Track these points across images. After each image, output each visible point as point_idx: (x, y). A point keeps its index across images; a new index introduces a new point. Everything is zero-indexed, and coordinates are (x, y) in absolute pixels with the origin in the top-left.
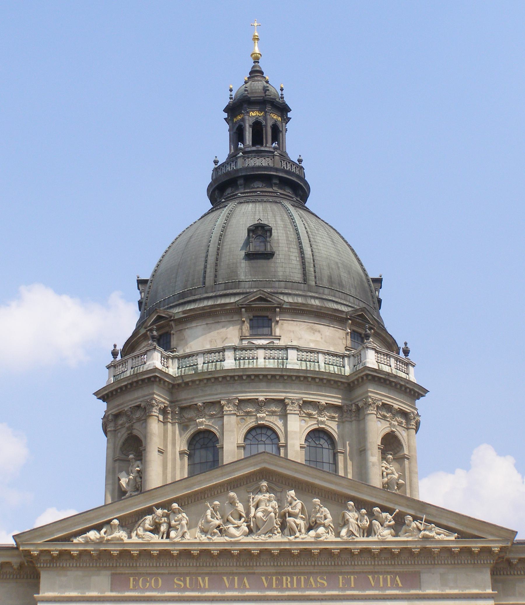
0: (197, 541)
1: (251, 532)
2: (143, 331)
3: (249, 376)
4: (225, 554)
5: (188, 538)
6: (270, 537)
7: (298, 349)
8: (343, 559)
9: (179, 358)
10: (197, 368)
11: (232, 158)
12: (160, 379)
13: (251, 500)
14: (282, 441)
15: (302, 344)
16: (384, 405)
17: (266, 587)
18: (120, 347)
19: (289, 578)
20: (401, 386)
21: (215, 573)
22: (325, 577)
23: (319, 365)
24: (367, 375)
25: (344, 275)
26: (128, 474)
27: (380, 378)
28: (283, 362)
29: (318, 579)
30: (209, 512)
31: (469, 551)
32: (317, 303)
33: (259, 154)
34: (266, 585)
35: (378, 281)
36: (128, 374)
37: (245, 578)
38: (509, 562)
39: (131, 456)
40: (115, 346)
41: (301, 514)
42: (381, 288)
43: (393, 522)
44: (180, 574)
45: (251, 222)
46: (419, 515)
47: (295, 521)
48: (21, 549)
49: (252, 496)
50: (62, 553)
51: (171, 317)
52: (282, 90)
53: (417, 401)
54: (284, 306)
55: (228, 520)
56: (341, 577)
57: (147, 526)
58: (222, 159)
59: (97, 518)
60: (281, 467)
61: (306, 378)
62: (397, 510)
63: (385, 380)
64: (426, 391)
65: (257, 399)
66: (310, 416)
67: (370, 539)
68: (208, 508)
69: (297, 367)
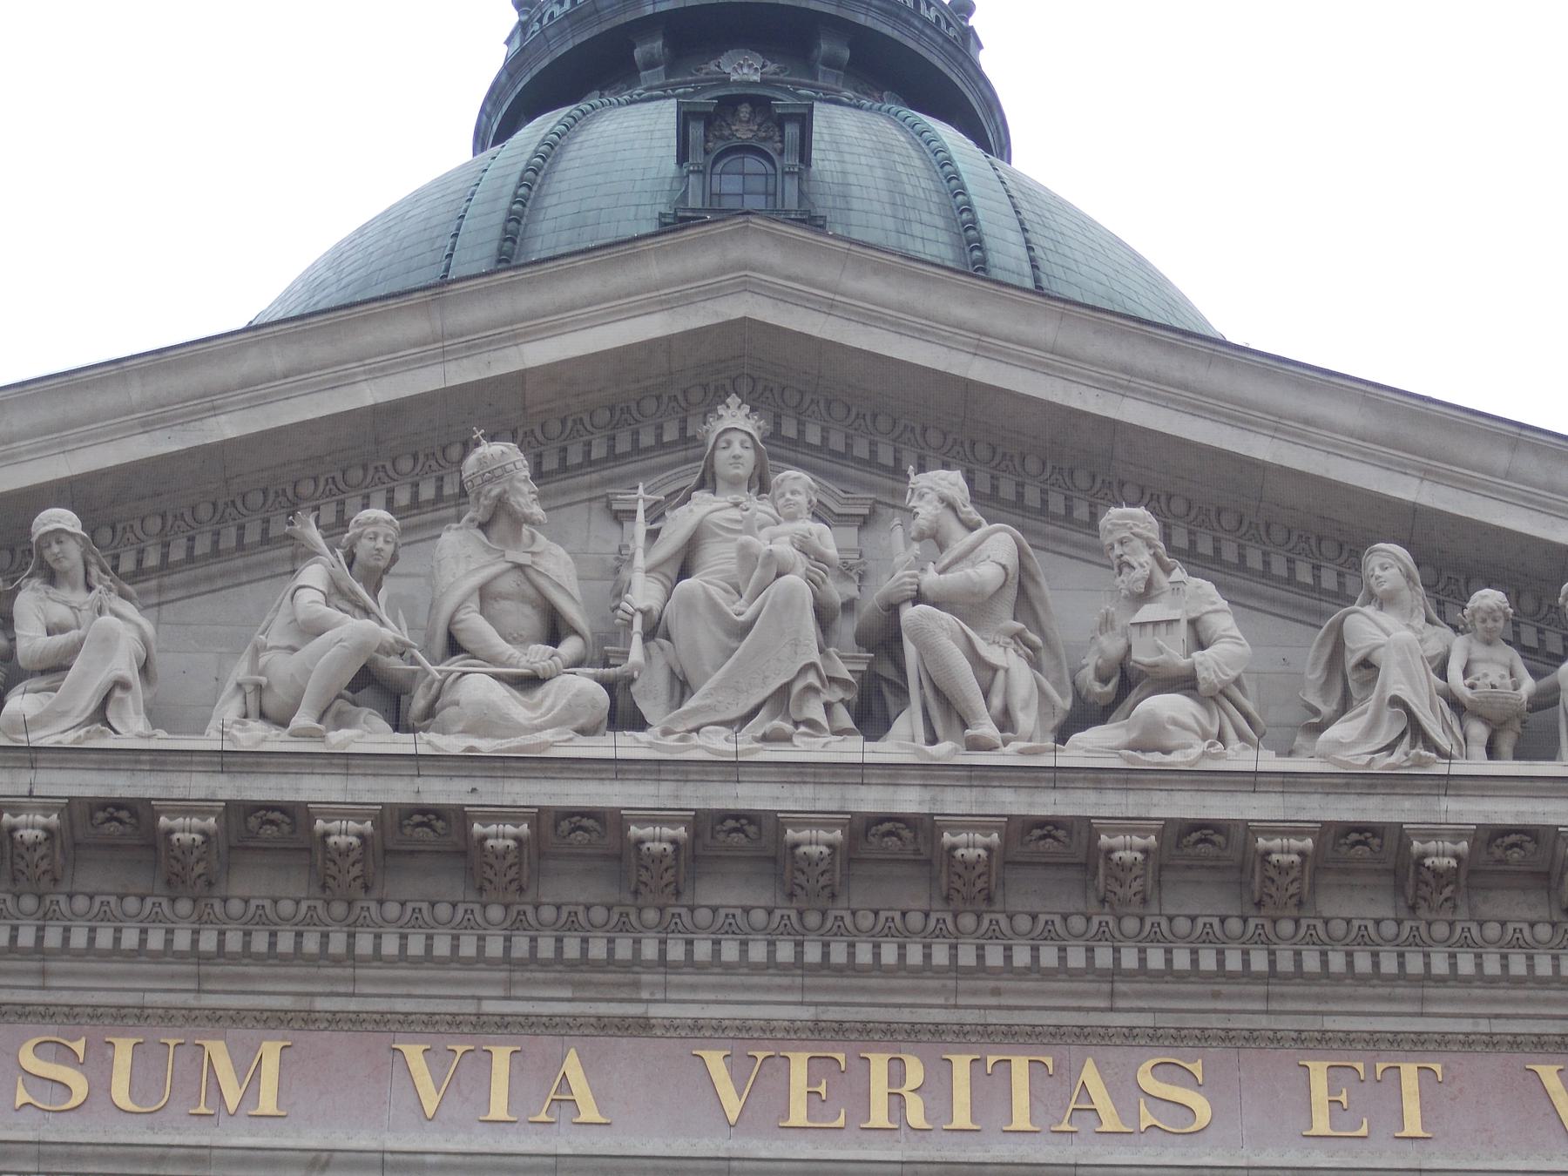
1: (624, 716)
6: (765, 738)
8: (1338, 928)
17: (732, 1118)
19: (915, 1072)
21: (334, 1020)
22: (1197, 1068)
29: (1147, 1082)
30: (313, 575)
34: (732, 1105)
37: (572, 1067)
41: (1015, 619)
47: (968, 637)
55: (454, 647)
60: (869, 318)
68: (310, 554)
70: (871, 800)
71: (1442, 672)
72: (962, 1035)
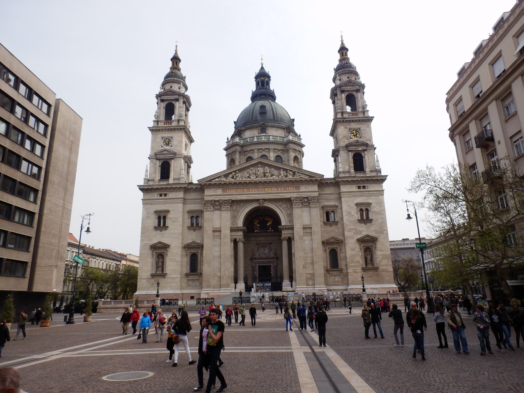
1: (257, 177)
2: (235, 134)
4: (250, 183)
5: (241, 179)
7: (272, 136)
9: (243, 139)
11: (256, 90)
14: (269, 158)
15: (274, 135)
16: (294, 149)
25: (284, 118)
33: (263, 88)
35: (293, 120)
38: (322, 183)
44: (239, 188)
45: (261, 105)
57: (231, 177)
59: (218, 175)
63: (294, 143)
64: (305, 146)
66: (276, 152)
67: (287, 178)
70: (265, 181)
72: (269, 187)
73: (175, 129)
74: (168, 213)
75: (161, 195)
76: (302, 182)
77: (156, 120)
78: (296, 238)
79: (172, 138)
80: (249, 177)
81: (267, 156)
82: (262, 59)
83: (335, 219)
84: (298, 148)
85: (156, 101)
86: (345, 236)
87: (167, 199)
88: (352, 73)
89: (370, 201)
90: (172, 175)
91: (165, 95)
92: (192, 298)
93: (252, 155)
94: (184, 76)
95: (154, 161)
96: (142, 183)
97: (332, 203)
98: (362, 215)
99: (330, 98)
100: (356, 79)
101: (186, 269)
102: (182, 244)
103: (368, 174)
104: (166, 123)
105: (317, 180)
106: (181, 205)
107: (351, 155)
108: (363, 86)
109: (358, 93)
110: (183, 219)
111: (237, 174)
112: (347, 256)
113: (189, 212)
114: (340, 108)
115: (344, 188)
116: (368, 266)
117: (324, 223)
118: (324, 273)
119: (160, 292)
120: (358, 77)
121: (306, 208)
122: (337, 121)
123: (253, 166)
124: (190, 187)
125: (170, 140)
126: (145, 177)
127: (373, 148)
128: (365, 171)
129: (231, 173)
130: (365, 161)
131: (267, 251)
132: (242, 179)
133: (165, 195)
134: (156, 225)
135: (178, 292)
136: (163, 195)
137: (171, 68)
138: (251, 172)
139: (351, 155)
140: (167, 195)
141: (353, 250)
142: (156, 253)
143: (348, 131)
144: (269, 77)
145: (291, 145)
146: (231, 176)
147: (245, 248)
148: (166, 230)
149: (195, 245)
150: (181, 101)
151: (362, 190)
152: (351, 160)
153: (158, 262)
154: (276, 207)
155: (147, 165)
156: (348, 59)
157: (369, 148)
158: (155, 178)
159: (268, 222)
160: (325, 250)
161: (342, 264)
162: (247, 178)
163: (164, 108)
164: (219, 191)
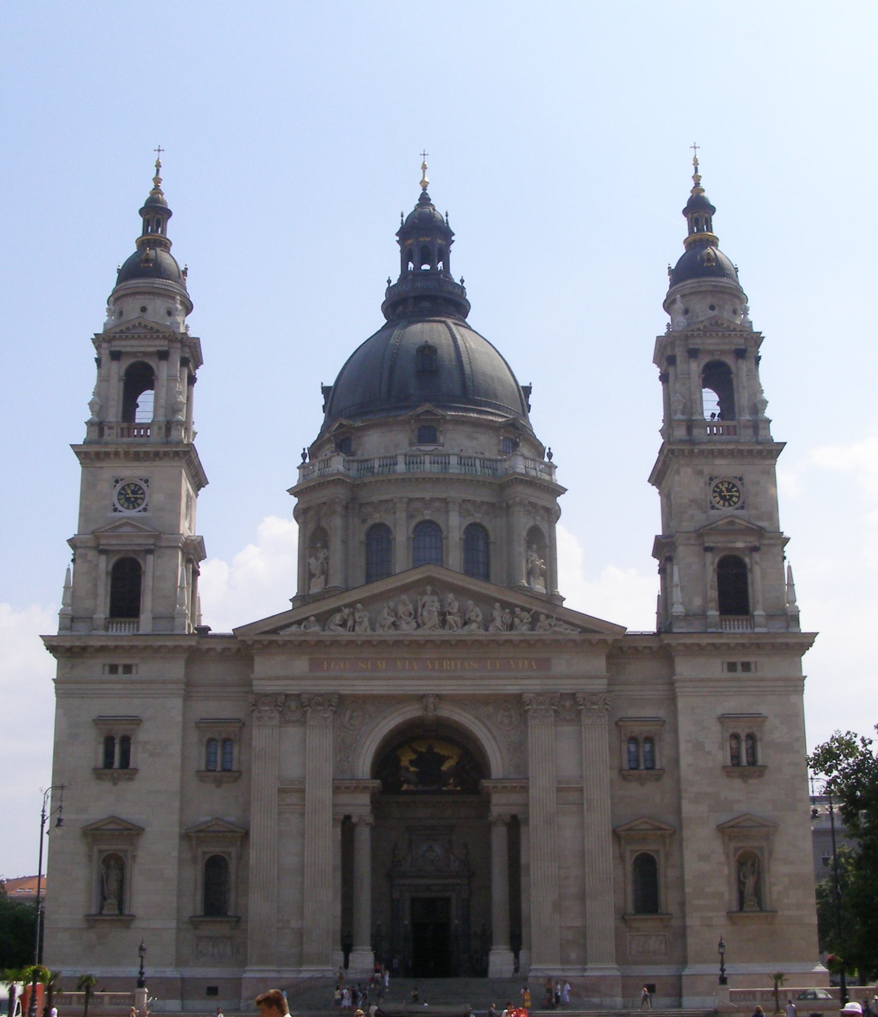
0: (377, 633)
1: (419, 626)
2: (327, 436)
3: (417, 479)
4: (397, 643)
9: (358, 461)
10: (374, 471)
12: (343, 481)
13: (419, 601)
16: (530, 502)
18: (306, 451)
19: (448, 663)
20: (545, 487)
23: (476, 469)
24: (516, 479)
26: (317, 559)
27: (526, 481)
28: (446, 466)
29: (472, 663)
31: (590, 642)
32: (476, 415)
34: (430, 667)
35: (527, 390)
36: (316, 474)
37: (414, 664)
38: (621, 648)
39: (319, 545)
40: (304, 449)
42: (530, 393)
43: (530, 620)
46: (551, 614)
48: (239, 638)
49: (419, 597)
50: (271, 642)
51: (351, 425)
52: (447, 216)
53: (558, 499)
54: (447, 418)
55: (401, 617)
56: (489, 662)
57: (337, 622)
58: (394, 281)
61: (465, 480)
62: (533, 611)
65: (423, 498)
67: (513, 632)
69: (457, 471)
70: (443, 638)
71: (502, 617)
73: (157, 454)
74: (134, 727)
75: (113, 669)
76: (557, 645)
77: (96, 420)
78: (536, 818)
79: (146, 481)
80: (394, 624)
81: (438, 526)
82: (424, 167)
83: (653, 761)
84: (540, 498)
85: (94, 353)
86: (683, 815)
87: (133, 682)
88: (724, 293)
89: (763, 709)
90: (147, 603)
91: (127, 337)
92: (212, 991)
93: (388, 521)
94: (182, 268)
95: (92, 555)
96: (53, 629)
97: (648, 712)
98: (735, 757)
99: (654, 362)
100: (735, 312)
101: (195, 904)
102: (181, 823)
103: (761, 626)
104: (126, 430)
105: (605, 641)
106: (178, 702)
107: (713, 563)
108: (758, 339)
109: (740, 361)
110: (184, 745)
111: (357, 615)
112: (686, 878)
113: (202, 724)
114: (685, 406)
115: (685, 668)
116: (745, 909)
117: (621, 770)
118: (616, 928)
119: (149, 972)
120: (743, 307)
121: (569, 728)
122: (672, 451)
123: (405, 588)
124: (205, 647)
125: (140, 488)
126: (62, 606)
127: (779, 542)
128: (753, 616)
129: (338, 610)
130: (753, 583)
131: (438, 850)
132: (373, 629)
133: (128, 669)
134: (100, 763)
135: (171, 972)
136: (120, 669)
137: (143, 243)
138: (401, 610)
139: (711, 561)
140: (134, 669)
141: (704, 858)
142: (100, 851)
143: (705, 483)
144: (447, 235)
145: (520, 488)
146: (337, 618)
147: (374, 840)
148: (130, 779)
149: (222, 829)
150: (176, 358)
151: (739, 674)
152: (711, 576)
153: (107, 880)
154: (477, 722)
155: (68, 570)
156: (713, 242)
157: (766, 542)
158: (94, 611)
159: (443, 759)
160: (622, 857)
161: (668, 899)
162: (389, 628)
163: (120, 380)
164: (301, 665)
